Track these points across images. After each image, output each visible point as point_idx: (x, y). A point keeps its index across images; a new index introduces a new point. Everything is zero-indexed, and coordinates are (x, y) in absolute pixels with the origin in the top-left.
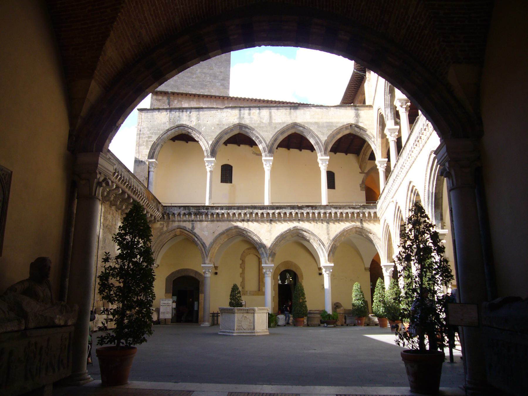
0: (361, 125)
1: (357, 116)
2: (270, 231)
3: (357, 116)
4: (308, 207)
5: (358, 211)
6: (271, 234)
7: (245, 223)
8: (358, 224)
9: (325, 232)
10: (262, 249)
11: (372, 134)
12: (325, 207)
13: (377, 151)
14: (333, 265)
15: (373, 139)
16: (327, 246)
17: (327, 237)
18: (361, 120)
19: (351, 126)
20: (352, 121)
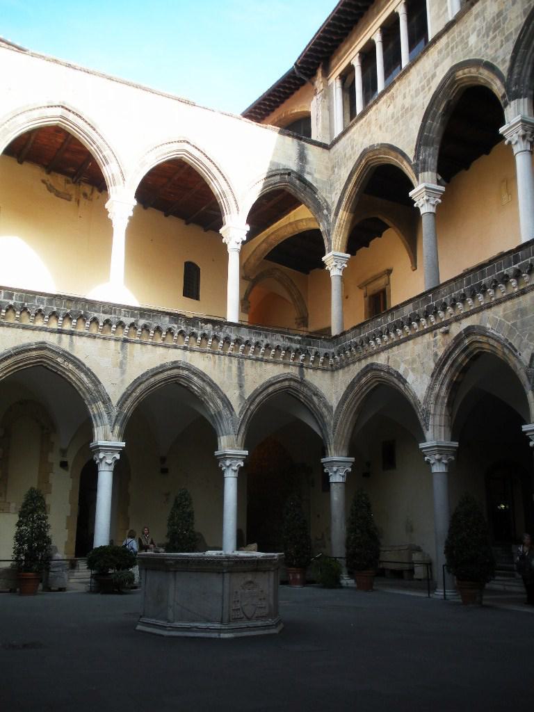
0: (308, 178)
1: (302, 157)
2: (122, 365)
3: (302, 157)
4: (207, 321)
5: (298, 346)
6: (123, 372)
7: (65, 338)
8: (293, 371)
9: (235, 380)
10: (100, 403)
11: (326, 201)
12: (238, 326)
13: (333, 238)
14: (246, 453)
15: (325, 212)
16: (237, 410)
17: (237, 392)
18: (308, 168)
19: (289, 174)
20: (293, 165)
